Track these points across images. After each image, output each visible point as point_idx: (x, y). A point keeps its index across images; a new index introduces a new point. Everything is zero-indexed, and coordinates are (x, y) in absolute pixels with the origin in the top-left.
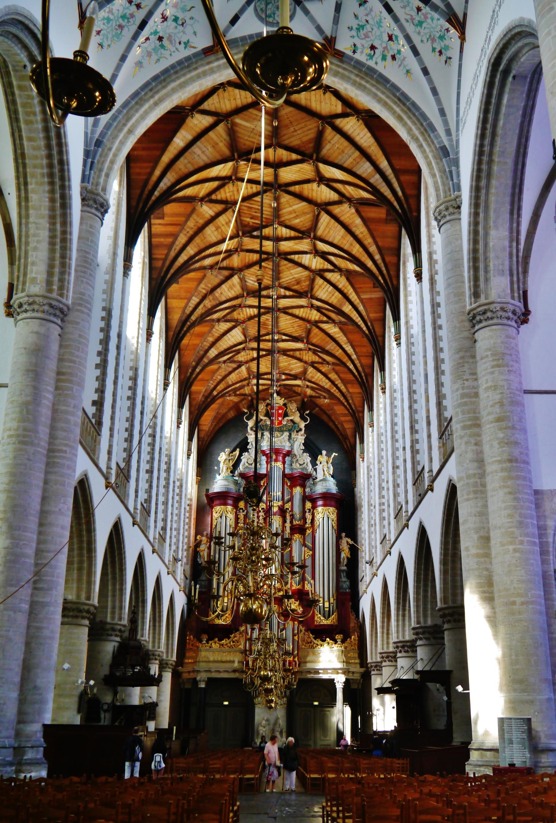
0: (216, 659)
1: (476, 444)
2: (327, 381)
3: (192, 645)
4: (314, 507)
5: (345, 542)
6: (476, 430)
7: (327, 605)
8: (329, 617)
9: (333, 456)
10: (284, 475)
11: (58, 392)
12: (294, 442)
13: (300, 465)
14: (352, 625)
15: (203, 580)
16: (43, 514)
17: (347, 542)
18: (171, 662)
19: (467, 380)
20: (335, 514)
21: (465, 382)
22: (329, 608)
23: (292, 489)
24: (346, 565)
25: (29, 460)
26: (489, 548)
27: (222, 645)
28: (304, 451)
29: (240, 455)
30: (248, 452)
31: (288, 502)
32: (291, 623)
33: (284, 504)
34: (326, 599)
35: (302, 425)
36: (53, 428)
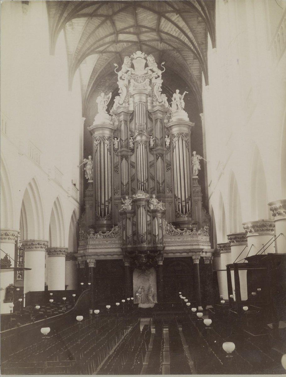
2: (177, 29)
5: (196, 159)
9: (184, 94)
12: (154, 86)
13: (159, 103)
17: (198, 158)
24: (197, 175)
27: (105, 236)
28: (162, 93)
29: (113, 98)
30: (119, 95)
34: (183, 199)
35: (160, 73)
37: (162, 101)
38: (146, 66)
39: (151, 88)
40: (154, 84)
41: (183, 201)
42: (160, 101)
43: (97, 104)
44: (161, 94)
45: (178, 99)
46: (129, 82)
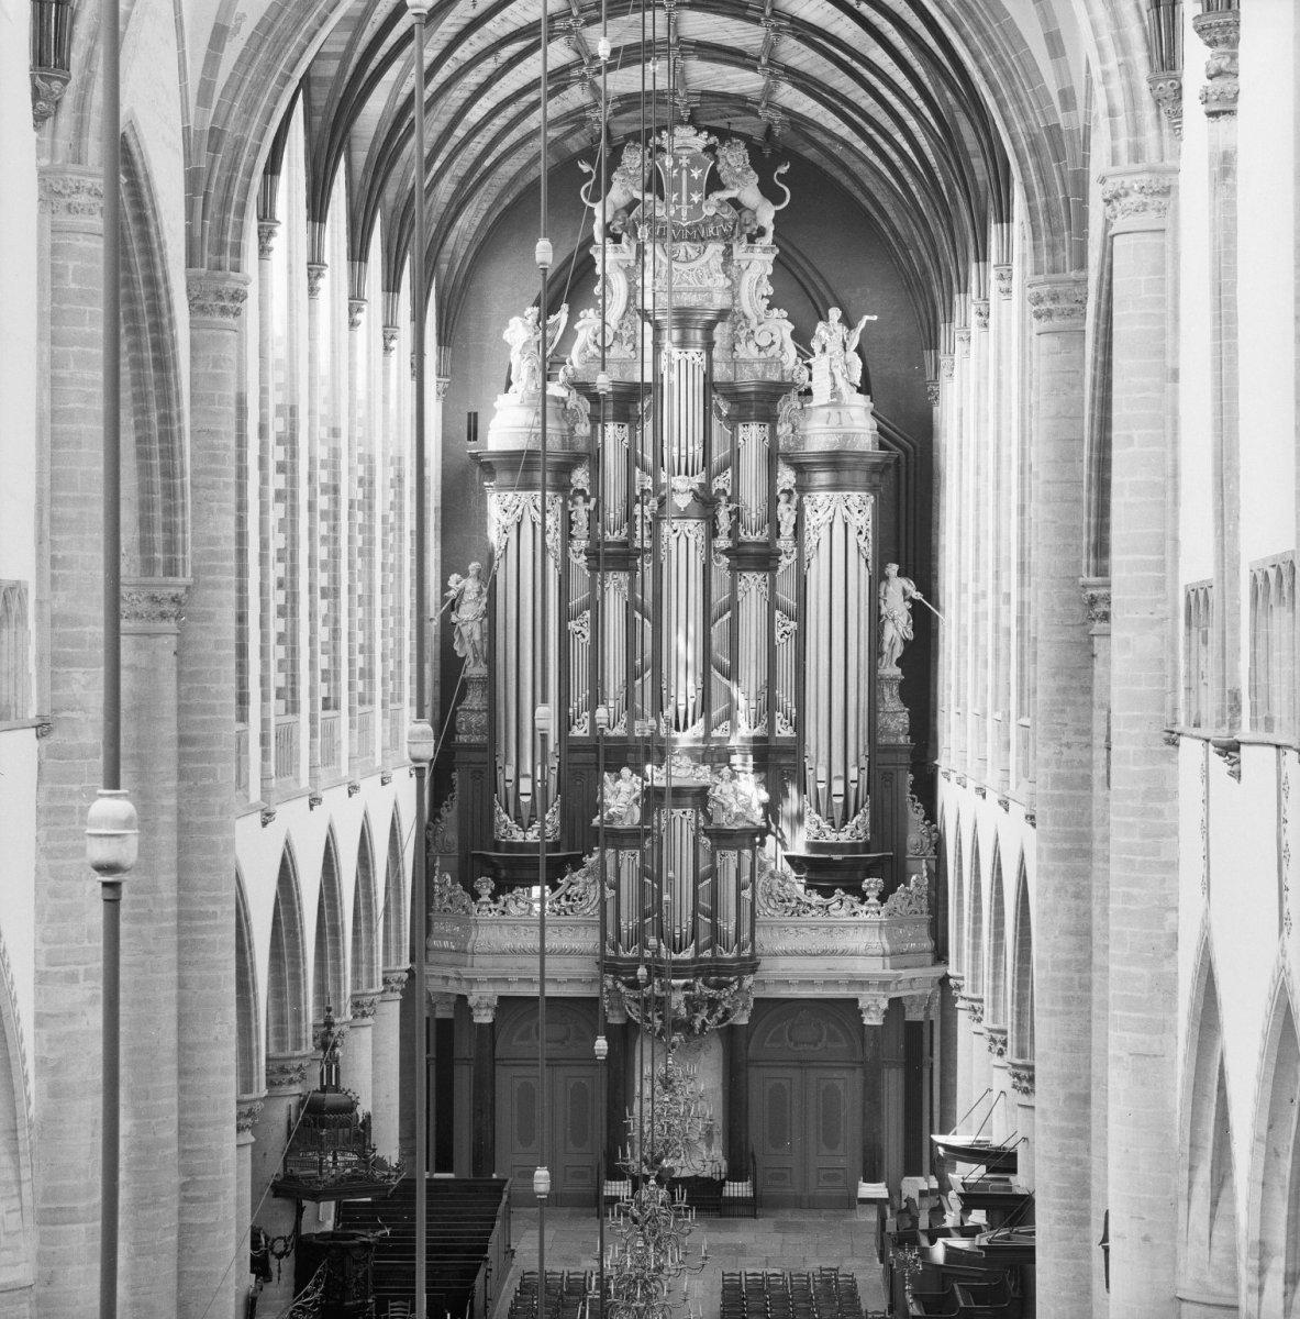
0: (519, 945)
1: (1077, 896)
3: (451, 902)
4: (802, 488)
6: (1079, 863)
7: (838, 787)
8: (845, 820)
9: (862, 325)
10: (710, 386)
11: (185, 783)
12: (741, 273)
13: (760, 349)
14: (913, 839)
15: (472, 711)
16: (184, 1049)
17: (905, 592)
18: (396, 976)
19: (1068, 745)
20: (868, 510)
21: (1064, 749)
22: (846, 795)
23: (733, 429)
24: (899, 663)
25: (150, 953)
26: (1087, 1118)
31: (722, 469)
32: (732, 855)
33: (710, 478)
34: (838, 770)
35: (766, 215)
36: (183, 867)
37: (773, 343)
38: (714, 183)
39: (729, 283)
40: (743, 266)
41: (838, 778)
42: (764, 342)
43: (508, 347)
44: (770, 307)
45: (834, 347)
46: (641, 251)
